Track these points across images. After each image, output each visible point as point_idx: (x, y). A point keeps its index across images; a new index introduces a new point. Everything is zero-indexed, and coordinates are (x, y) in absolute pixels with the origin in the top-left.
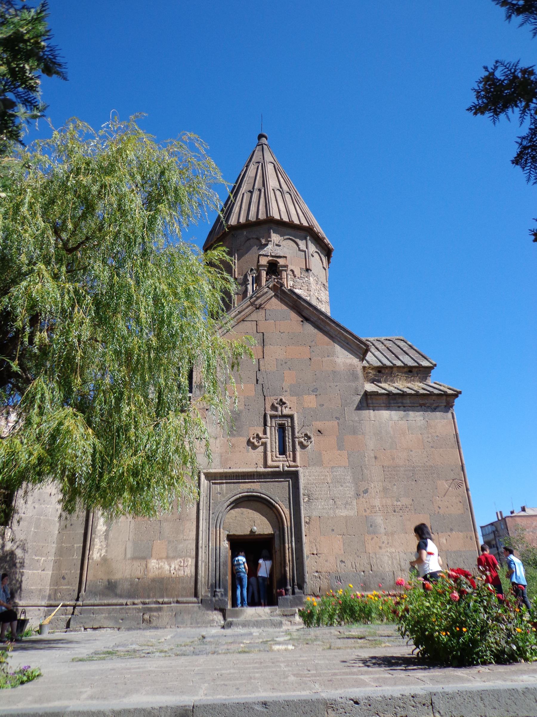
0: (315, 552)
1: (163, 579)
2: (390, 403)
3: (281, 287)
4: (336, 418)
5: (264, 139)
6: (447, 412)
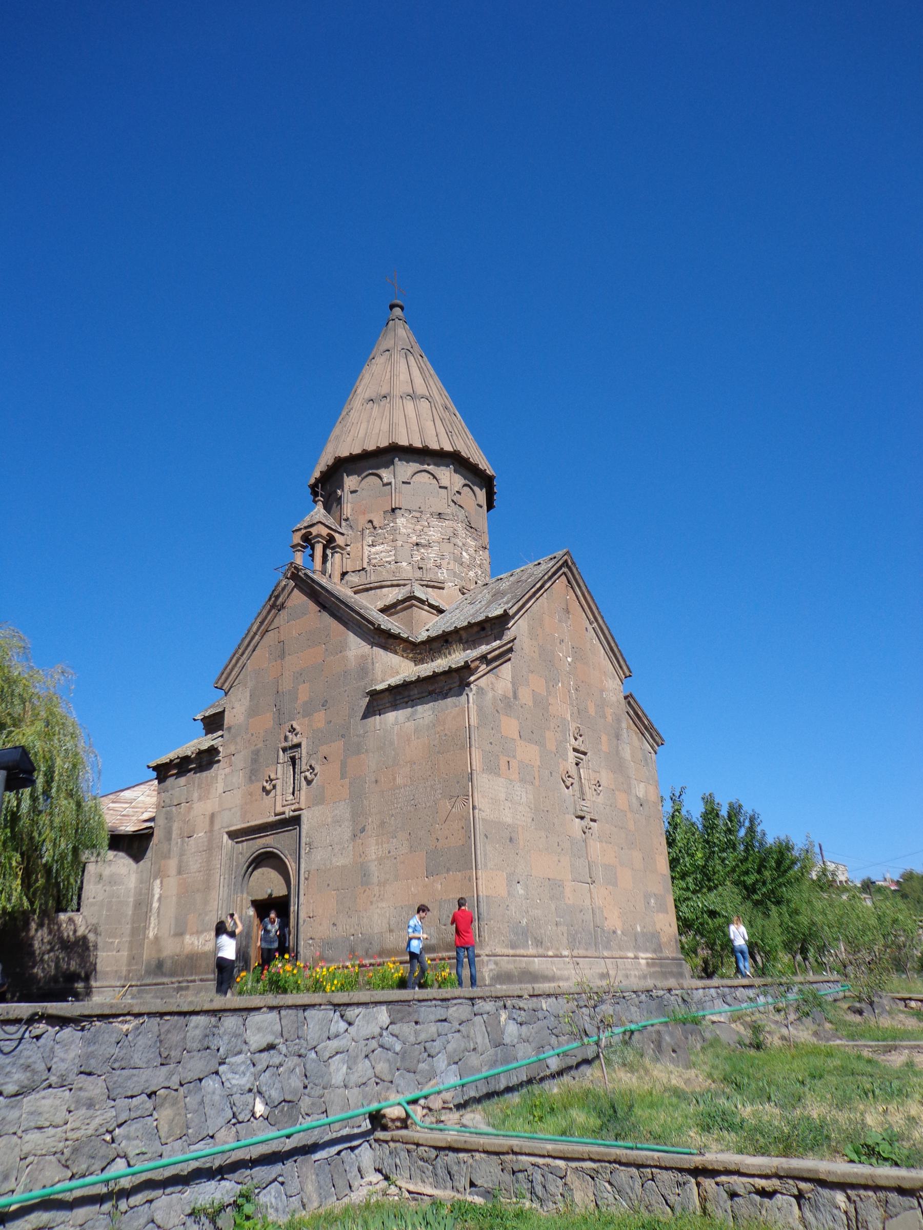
0: (311, 915)
1: (193, 955)
2: (396, 700)
3: (298, 572)
4: (343, 736)
5: (398, 309)
6: (460, 694)
